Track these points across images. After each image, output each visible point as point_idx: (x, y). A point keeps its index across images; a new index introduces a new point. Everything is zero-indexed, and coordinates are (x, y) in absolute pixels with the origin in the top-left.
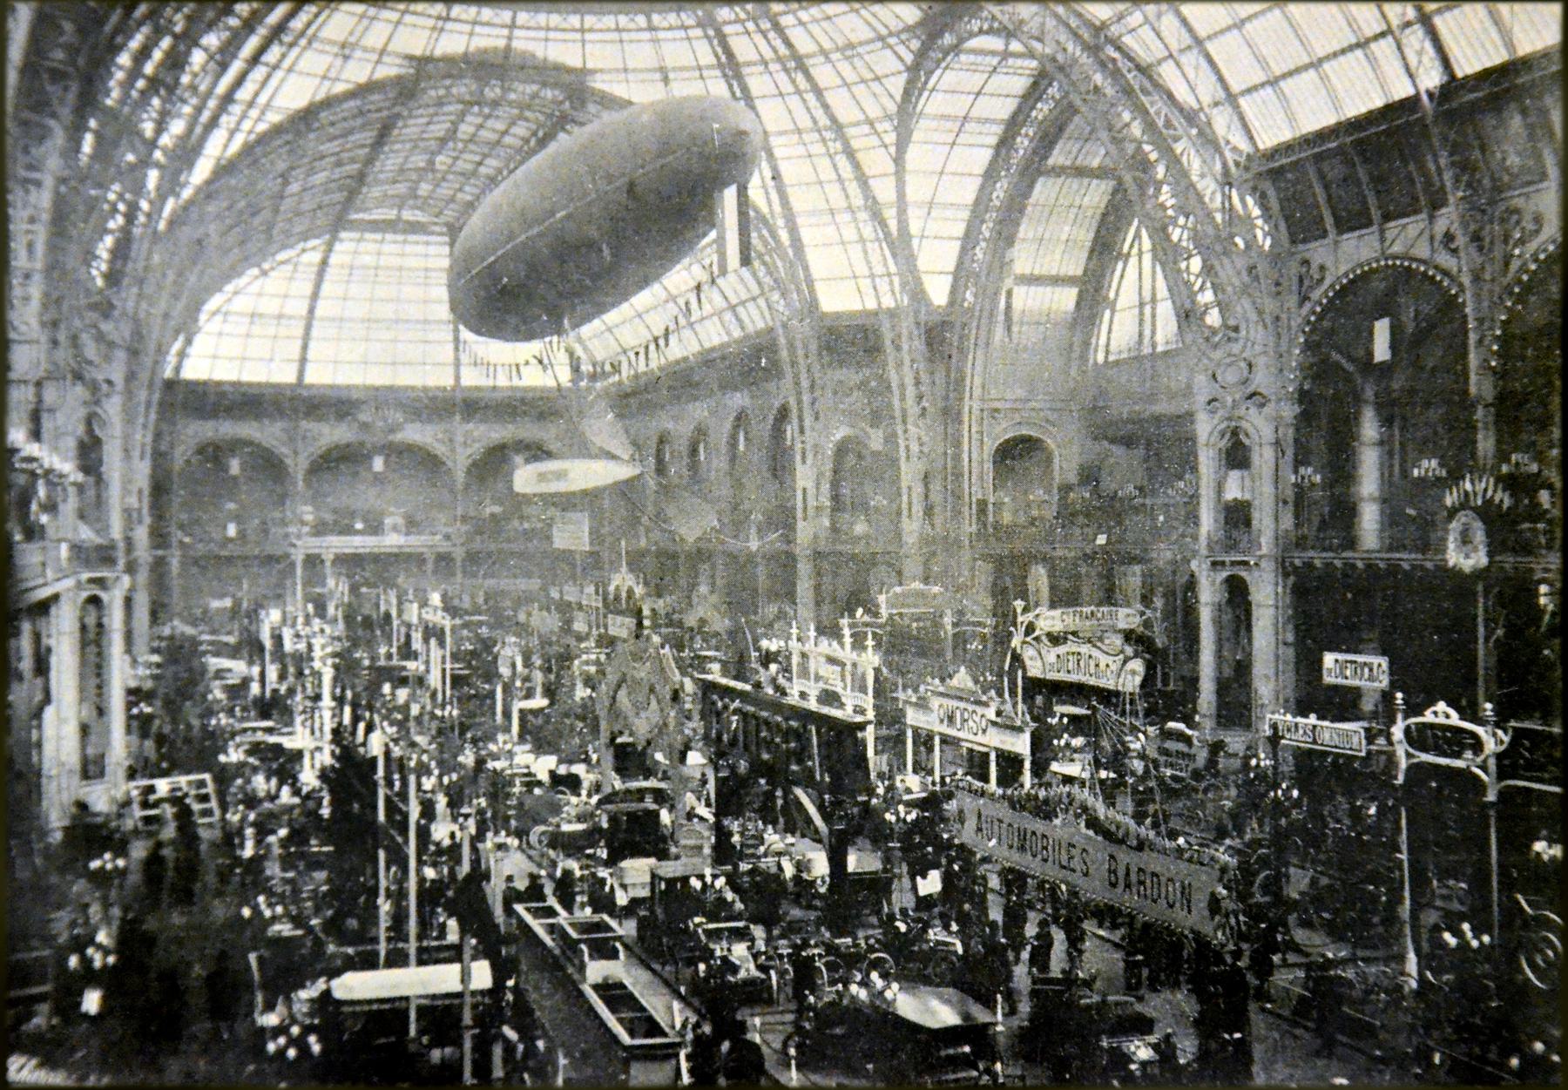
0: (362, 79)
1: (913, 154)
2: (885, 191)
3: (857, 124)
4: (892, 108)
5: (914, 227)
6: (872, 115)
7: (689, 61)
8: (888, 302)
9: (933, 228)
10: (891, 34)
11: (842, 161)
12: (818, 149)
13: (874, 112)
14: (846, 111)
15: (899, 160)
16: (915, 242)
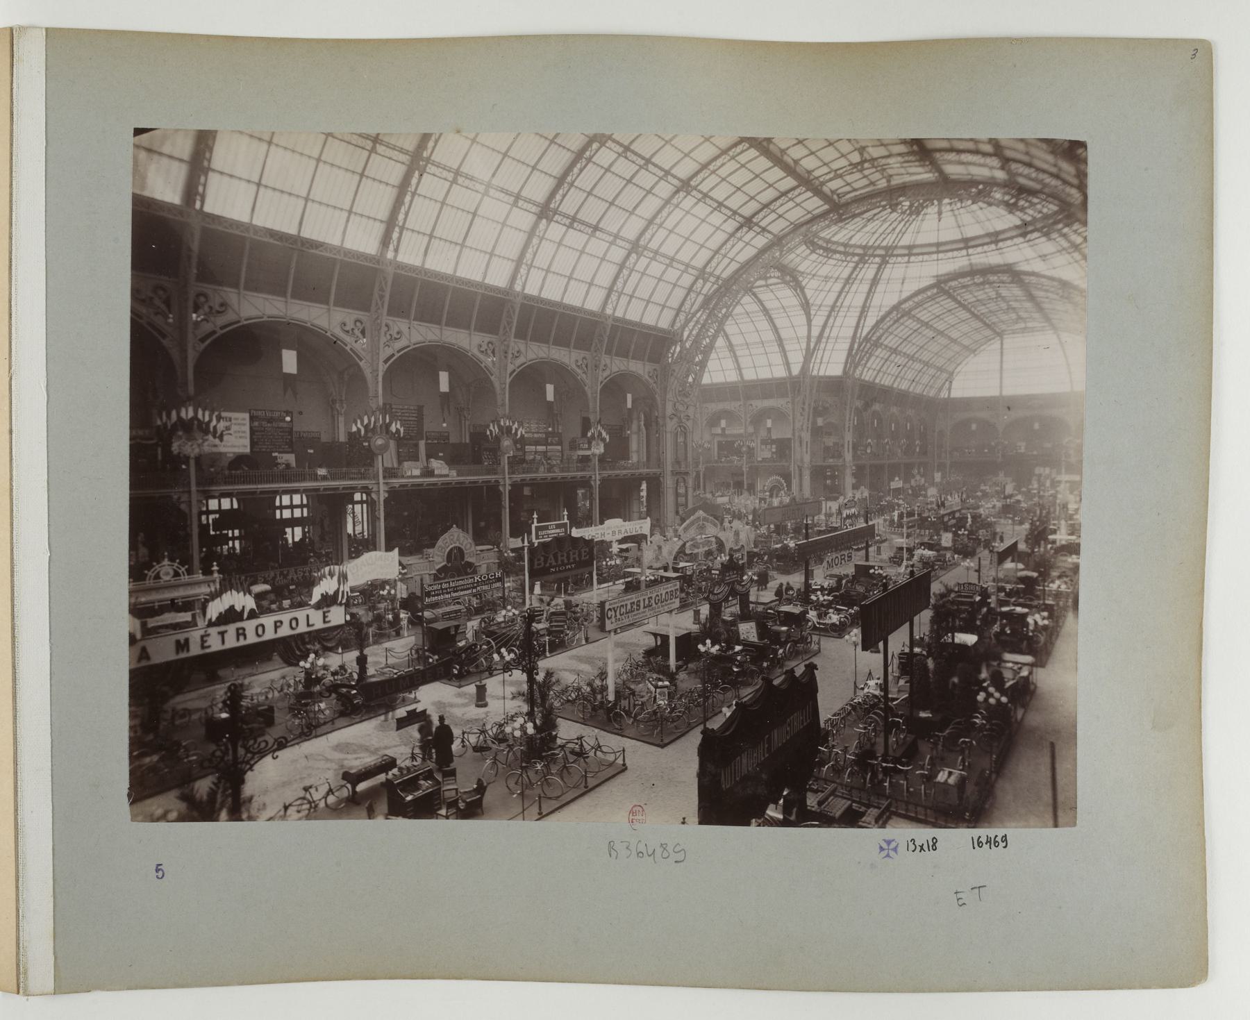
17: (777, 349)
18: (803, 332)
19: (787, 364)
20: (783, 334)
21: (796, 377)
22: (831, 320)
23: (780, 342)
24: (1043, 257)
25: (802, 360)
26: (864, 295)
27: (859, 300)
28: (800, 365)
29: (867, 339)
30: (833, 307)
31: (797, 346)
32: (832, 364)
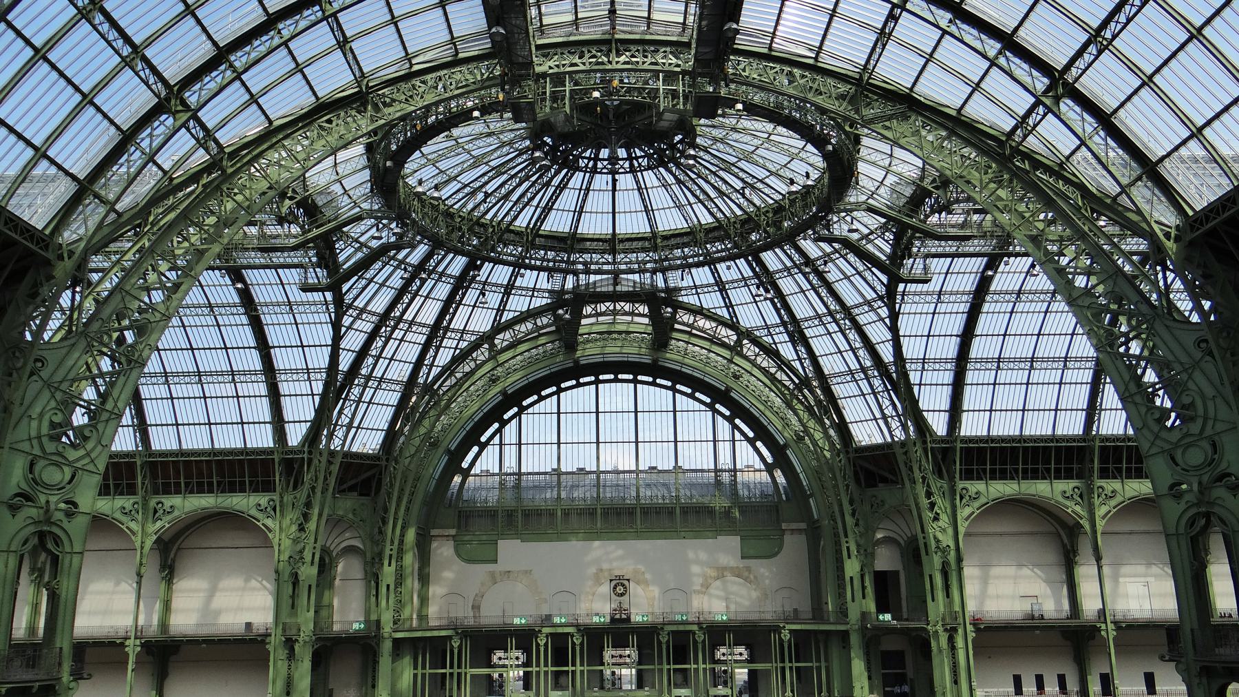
0: (525, 309)
1: (904, 325)
2: (887, 353)
3: (861, 305)
4: (882, 290)
5: (914, 377)
6: (869, 298)
7: (736, 276)
8: (899, 434)
9: (928, 377)
10: (872, 233)
11: (852, 335)
12: (833, 327)
13: (870, 295)
14: (851, 298)
15: (894, 329)
16: (916, 389)
17: (262, 389)
18: (321, 359)
19: (278, 422)
20: (282, 360)
21: (293, 451)
22: (379, 343)
23: (269, 370)
24: (721, 286)
25: (310, 415)
26: (439, 305)
27: (429, 313)
28: (304, 428)
29: (428, 388)
30: (385, 316)
31: (304, 388)
32: (367, 429)
